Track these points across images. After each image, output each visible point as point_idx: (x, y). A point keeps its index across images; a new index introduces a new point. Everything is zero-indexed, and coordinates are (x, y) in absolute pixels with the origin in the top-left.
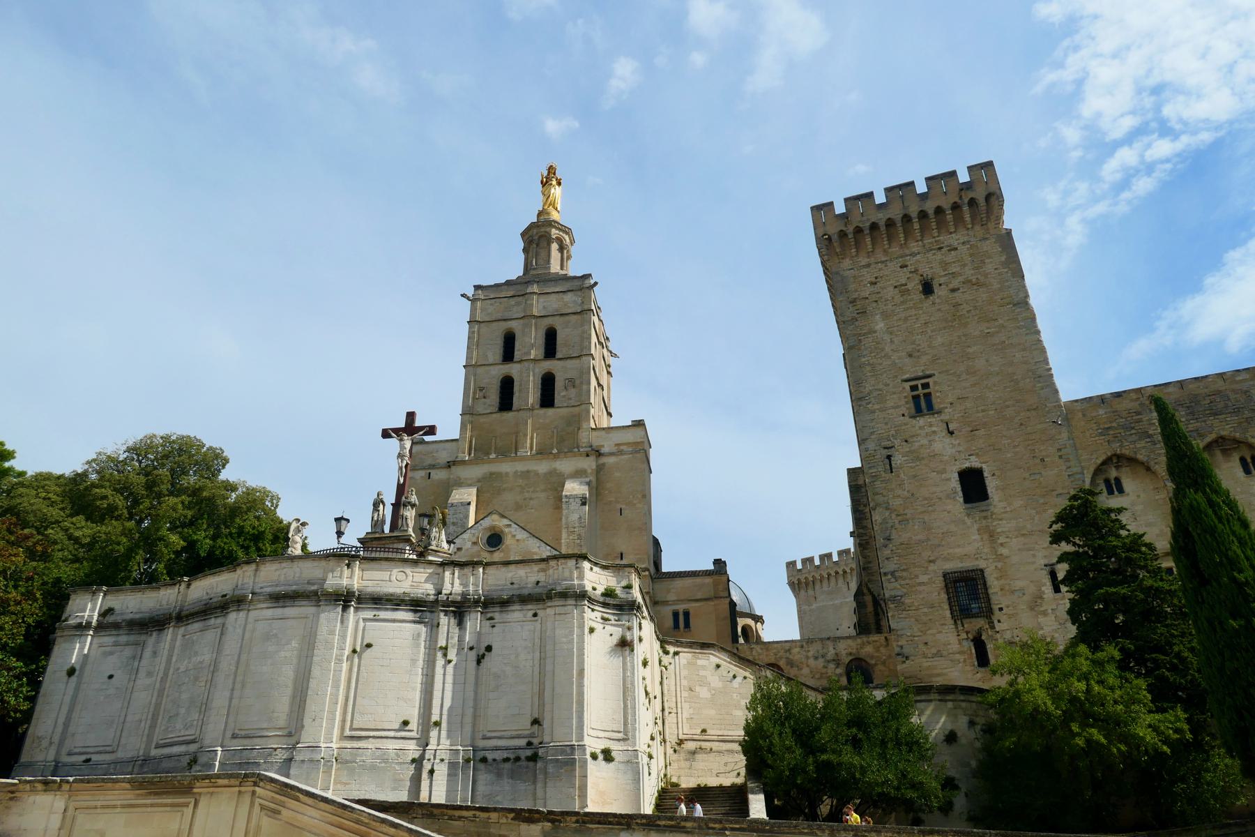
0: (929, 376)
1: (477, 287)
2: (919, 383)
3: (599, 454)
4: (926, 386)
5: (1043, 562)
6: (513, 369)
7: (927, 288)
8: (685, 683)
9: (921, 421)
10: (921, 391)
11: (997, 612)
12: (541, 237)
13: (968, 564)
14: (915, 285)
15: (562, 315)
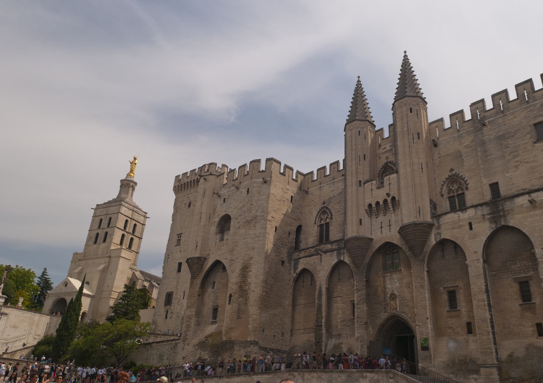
0: (181, 234)
1: (97, 205)
2: (179, 235)
3: (110, 257)
4: (181, 236)
5: (183, 290)
6: (99, 231)
7: (189, 206)
8: (54, 325)
9: (177, 247)
10: (180, 238)
11: (172, 304)
12: (123, 184)
13: (171, 290)
14: (187, 205)
15: (113, 214)
